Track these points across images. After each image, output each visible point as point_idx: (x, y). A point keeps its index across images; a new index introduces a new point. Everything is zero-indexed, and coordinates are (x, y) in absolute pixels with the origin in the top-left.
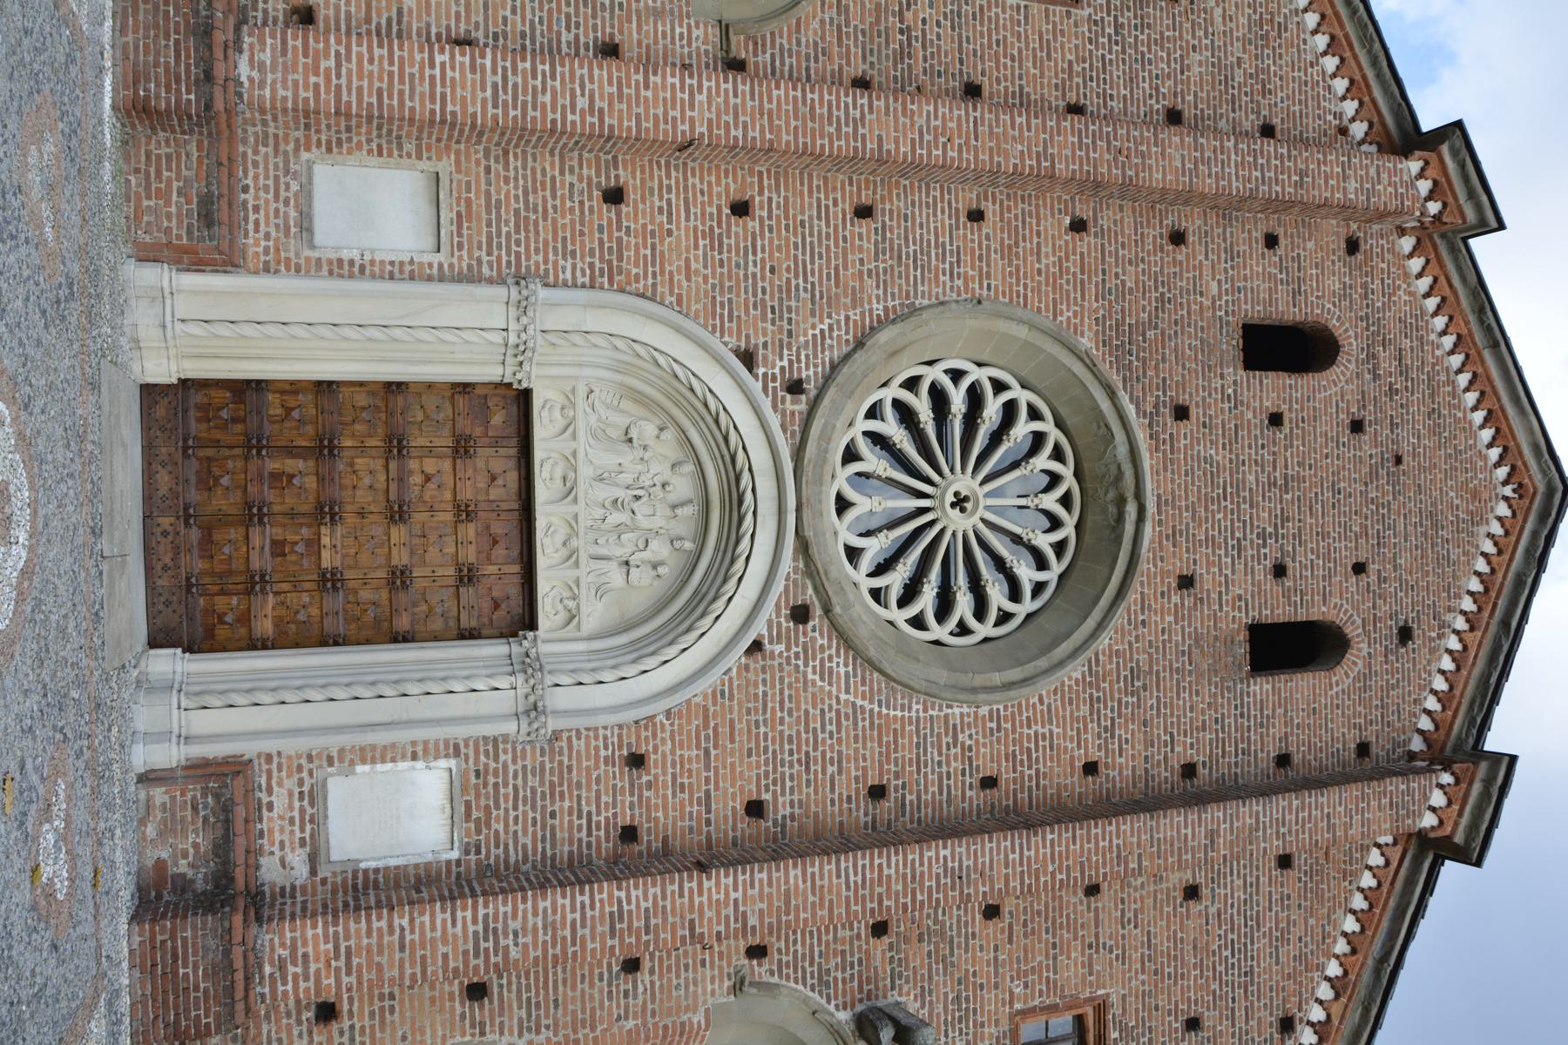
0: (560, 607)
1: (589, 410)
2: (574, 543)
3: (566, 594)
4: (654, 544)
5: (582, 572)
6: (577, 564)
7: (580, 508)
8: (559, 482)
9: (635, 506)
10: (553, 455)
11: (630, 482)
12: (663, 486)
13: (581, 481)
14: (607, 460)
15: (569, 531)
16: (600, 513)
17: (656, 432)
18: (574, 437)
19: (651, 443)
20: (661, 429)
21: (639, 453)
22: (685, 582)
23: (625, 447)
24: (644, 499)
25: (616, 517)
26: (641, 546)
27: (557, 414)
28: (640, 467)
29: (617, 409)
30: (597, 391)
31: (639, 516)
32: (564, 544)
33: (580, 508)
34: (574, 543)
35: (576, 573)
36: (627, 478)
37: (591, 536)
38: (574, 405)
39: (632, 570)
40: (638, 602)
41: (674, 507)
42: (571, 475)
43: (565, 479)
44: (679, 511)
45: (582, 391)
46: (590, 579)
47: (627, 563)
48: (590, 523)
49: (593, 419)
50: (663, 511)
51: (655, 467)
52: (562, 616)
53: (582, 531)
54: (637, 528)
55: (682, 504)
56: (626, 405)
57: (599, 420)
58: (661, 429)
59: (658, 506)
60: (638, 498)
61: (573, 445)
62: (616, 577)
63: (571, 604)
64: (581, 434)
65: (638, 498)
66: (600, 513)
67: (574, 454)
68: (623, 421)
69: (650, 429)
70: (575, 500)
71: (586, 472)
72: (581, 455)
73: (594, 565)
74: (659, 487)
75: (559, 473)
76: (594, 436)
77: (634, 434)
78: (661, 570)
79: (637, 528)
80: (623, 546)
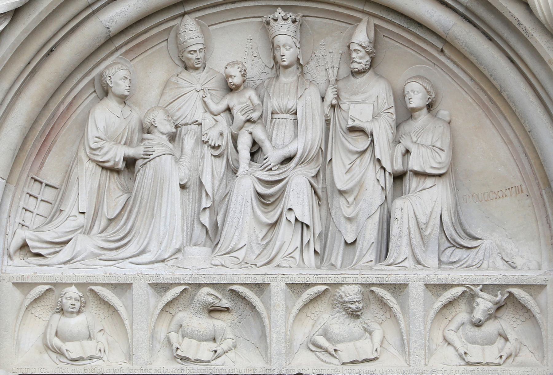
0: (491, 328)
1: (66, 253)
2: (351, 293)
3: (461, 314)
4: (359, 112)
5: (415, 277)
6: (397, 288)
7: (277, 278)
8: (220, 323)
9: (273, 155)
10: (162, 335)
11: (221, 165)
12: (231, 89)
13: (219, 275)
14: (171, 214)
15: (323, 307)
16: (286, 234)
17: (111, 104)
18: (122, 287)
19: (134, 116)
20: (106, 92)
21: (158, 142)
22: (445, 42)
23: (145, 174)
24: (259, 133)
25: (298, 198)
26: (362, 143)
27: (75, 323)
28: (189, 142)
29: (62, 190)
30: (23, 234)
31: (297, 146)
32: (354, 315)
33: (277, 278)
34: (351, 293)
35: (416, 291)
36: (211, 171)
37: (337, 254)
38: (55, 287)
39: (414, 164)
40: (490, 153)
41: (278, 67)
42: (205, 295)
43: (213, 310)
44: (288, 55)
45: (23, 268)
46: (432, 260)
47: (399, 177)
48: (309, 256)
49: (84, 244)
50: (285, 94)
51: (190, 108)
52: (507, 322)
53: (327, 275)
54: (323, 151)
55: (273, 47)
56: (51, 171)
57: (87, 230)
58: (106, 92)
59: (275, 103)
60: (256, 150)
61: (141, 290)
62: (427, 202)
63: (485, 303)
64: (118, 272)
65: (256, 150)
66: (286, 234)
67: (160, 287)
68: (88, 178)
69: (105, 118)
70: (260, 287)
71: (199, 263)
72: (164, 273)
73: (400, 248)
74: (234, 101)
75: (203, 324)
76: (122, 243)
77: (116, 154)
78: (416, 100)
79: (323, 151)
80: (360, 184)
